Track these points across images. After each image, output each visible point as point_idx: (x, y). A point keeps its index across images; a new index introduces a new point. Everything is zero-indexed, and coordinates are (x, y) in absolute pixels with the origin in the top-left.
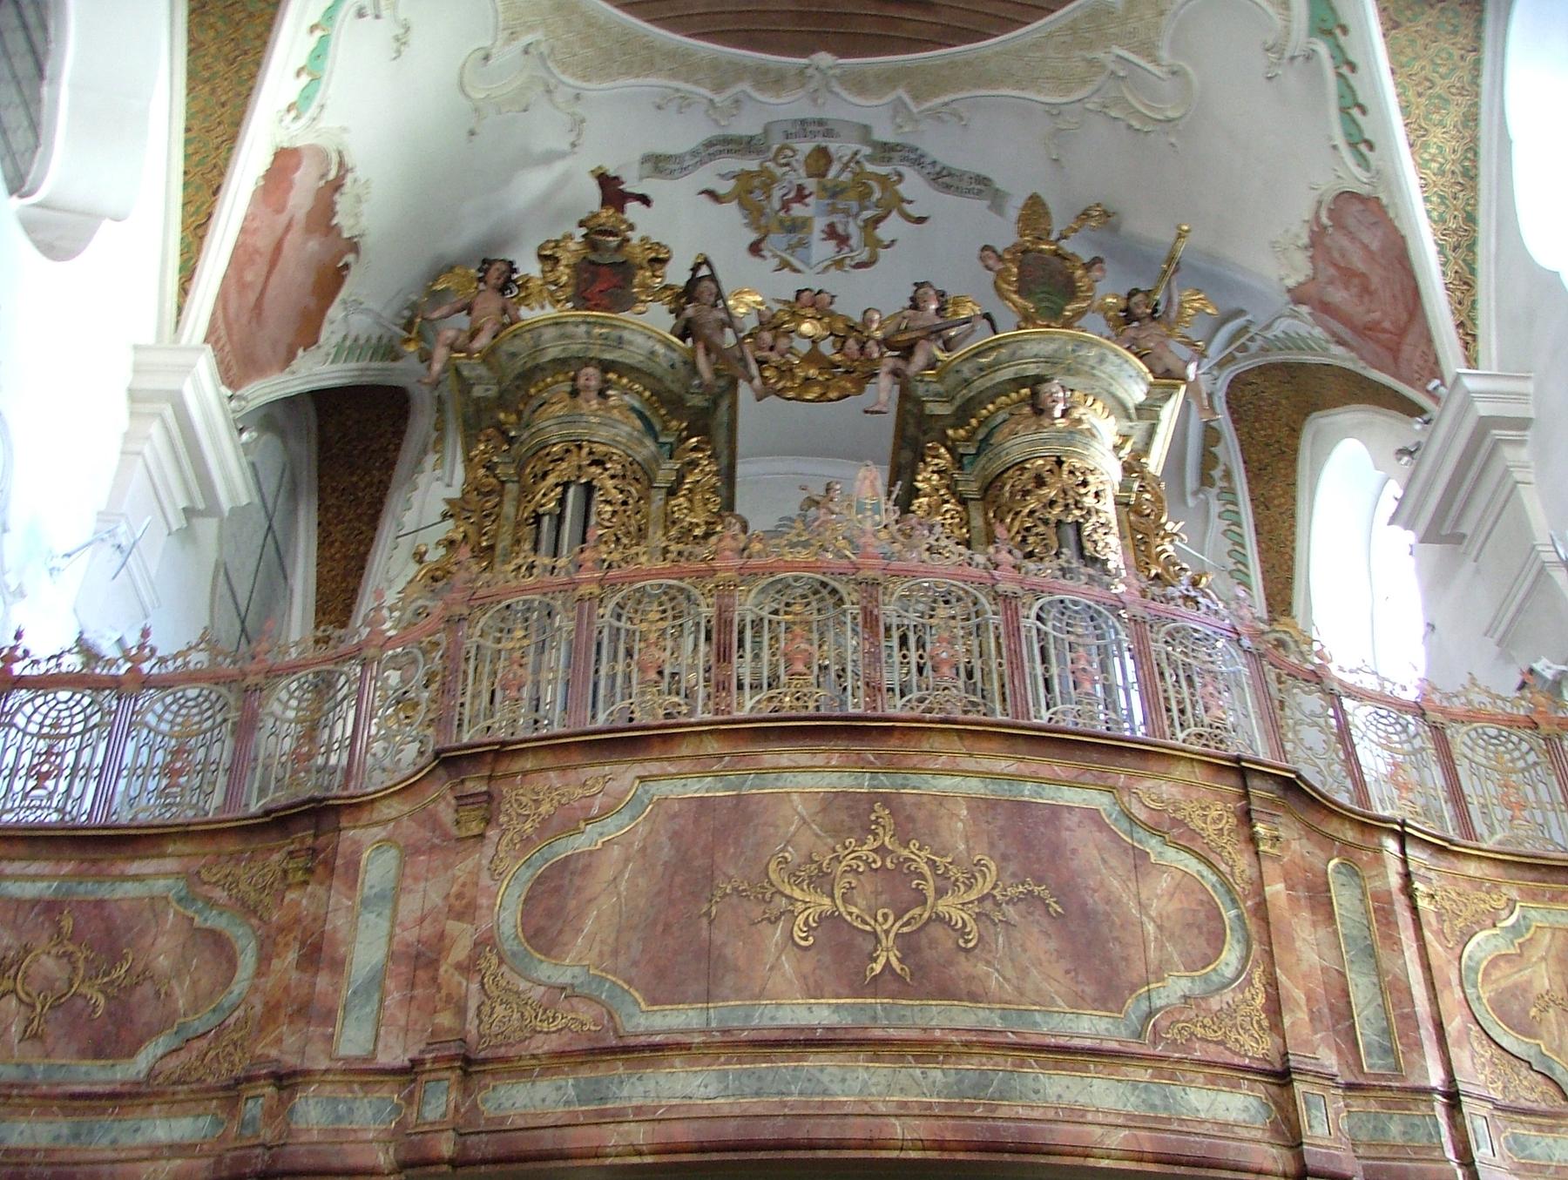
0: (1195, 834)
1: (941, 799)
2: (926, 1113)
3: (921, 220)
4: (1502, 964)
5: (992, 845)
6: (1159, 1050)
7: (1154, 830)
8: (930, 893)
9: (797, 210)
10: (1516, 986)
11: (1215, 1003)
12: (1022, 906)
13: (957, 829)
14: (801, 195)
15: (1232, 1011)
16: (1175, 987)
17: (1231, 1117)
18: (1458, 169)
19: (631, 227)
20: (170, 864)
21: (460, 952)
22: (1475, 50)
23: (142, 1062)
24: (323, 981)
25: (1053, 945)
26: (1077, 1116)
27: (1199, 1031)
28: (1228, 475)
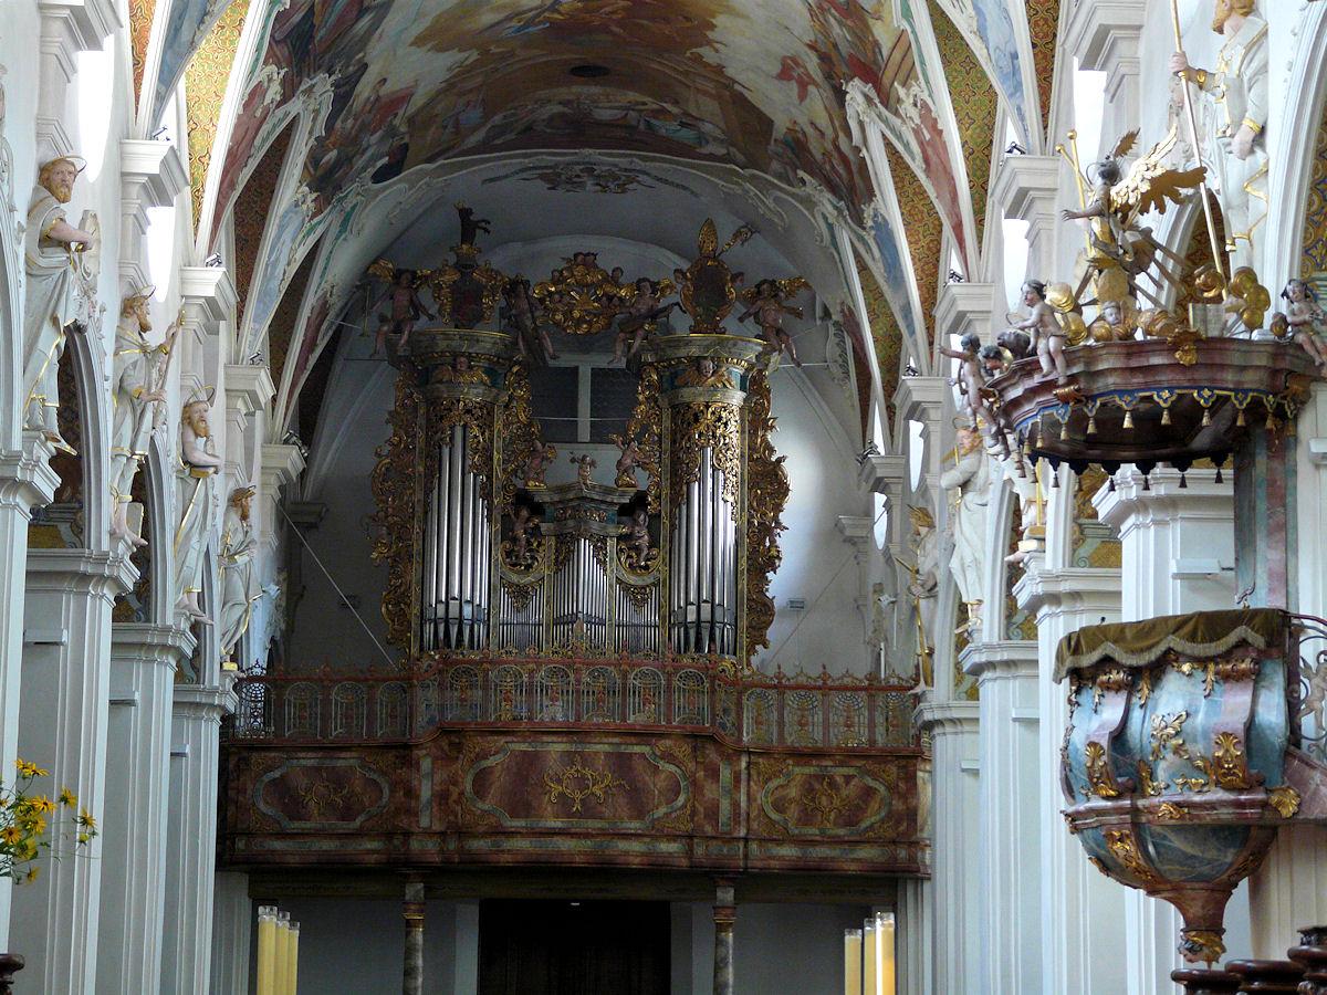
0: (676, 758)
1: (596, 753)
4: (780, 789)
6: (653, 832)
11: (673, 815)
13: (600, 761)
14: (578, 176)
15: (678, 817)
16: (662, 810)
20: (354, 754)
21: (455, 796)
23: (358, 822)
24: (413, 803)
25: (626, 800)
26: (627, 853)
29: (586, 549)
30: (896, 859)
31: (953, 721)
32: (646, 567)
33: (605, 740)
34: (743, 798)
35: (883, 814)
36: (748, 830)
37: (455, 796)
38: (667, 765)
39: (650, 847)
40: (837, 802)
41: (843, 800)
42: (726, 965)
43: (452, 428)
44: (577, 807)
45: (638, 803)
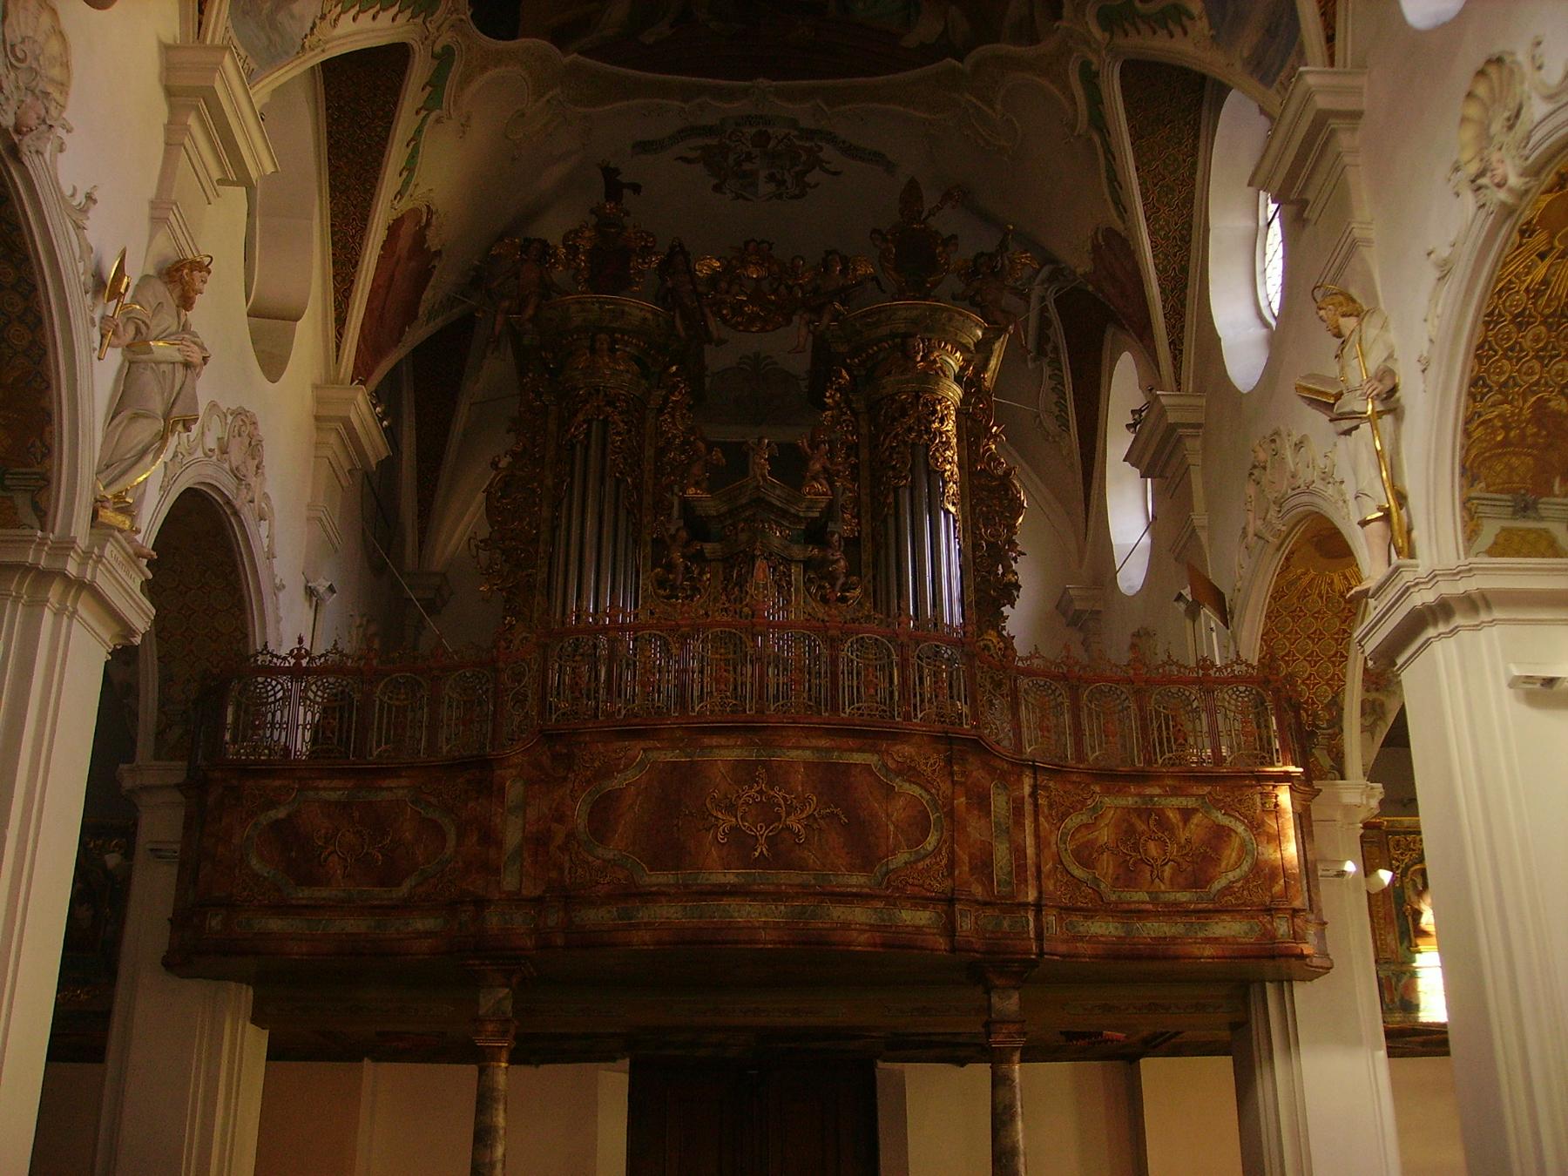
1: (791, 763)
2: (776, 926)
3: (835, 173)
4: (1083, 829)
5: (815, 787)
7: (899, 773)
8: (784, 815)
9: (747, 166)
10: (1088, 841)
11: (920, 865)
12: (827, 820)
13: (799, 777)
14: (749, 157)
15: (928, 869)
16: (902, 857)
17: (923, 922)
18: (1177, 235)
19: (627, 214)
20: (404, 782)
21: (559, 838)
22: (1193, 155)
23: (404, 889)
26: (846, 926)
27: (911, 881)
28: (1056, 349)
29: (762, 572)
30: (1274, 937)
31: (1475, 603)
32: (844, 599)
33: (806, 743)
34: (1030, 841)
35: (1245, 867)
36: (1040, 893)
37: (559, 838)
38: (906, 785)
39: (886, 917)
40: (1173, 849)
41: (1181, 847)
42: (1013, 1117)
43: (589, 422)
44: (761, 849)
45: (865, 853)
